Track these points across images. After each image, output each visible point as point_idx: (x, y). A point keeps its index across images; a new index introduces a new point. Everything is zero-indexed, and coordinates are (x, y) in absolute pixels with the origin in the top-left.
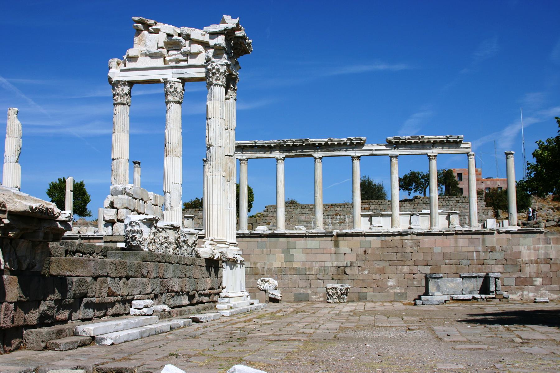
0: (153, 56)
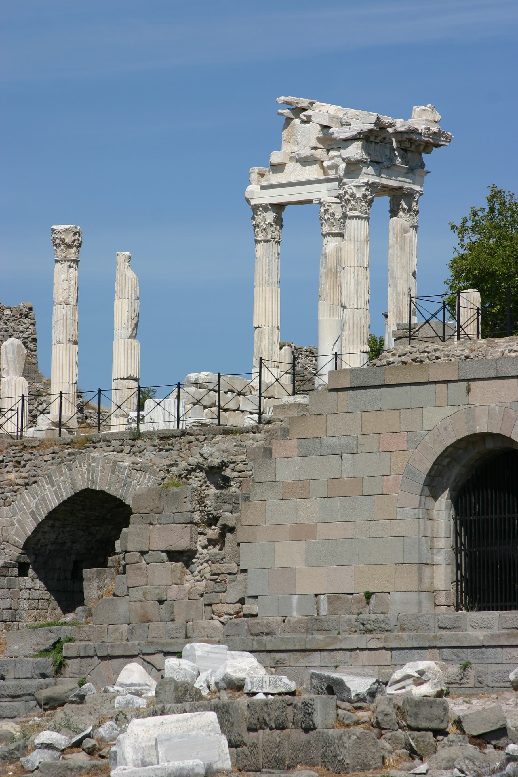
0: (306, 161)
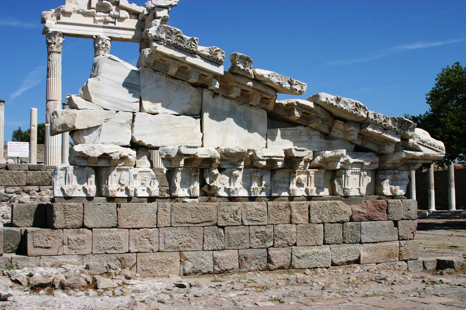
0: (85, 14)
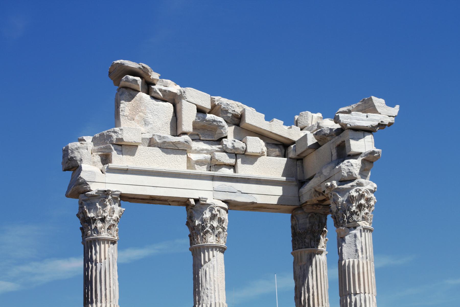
0: (168, 148)
